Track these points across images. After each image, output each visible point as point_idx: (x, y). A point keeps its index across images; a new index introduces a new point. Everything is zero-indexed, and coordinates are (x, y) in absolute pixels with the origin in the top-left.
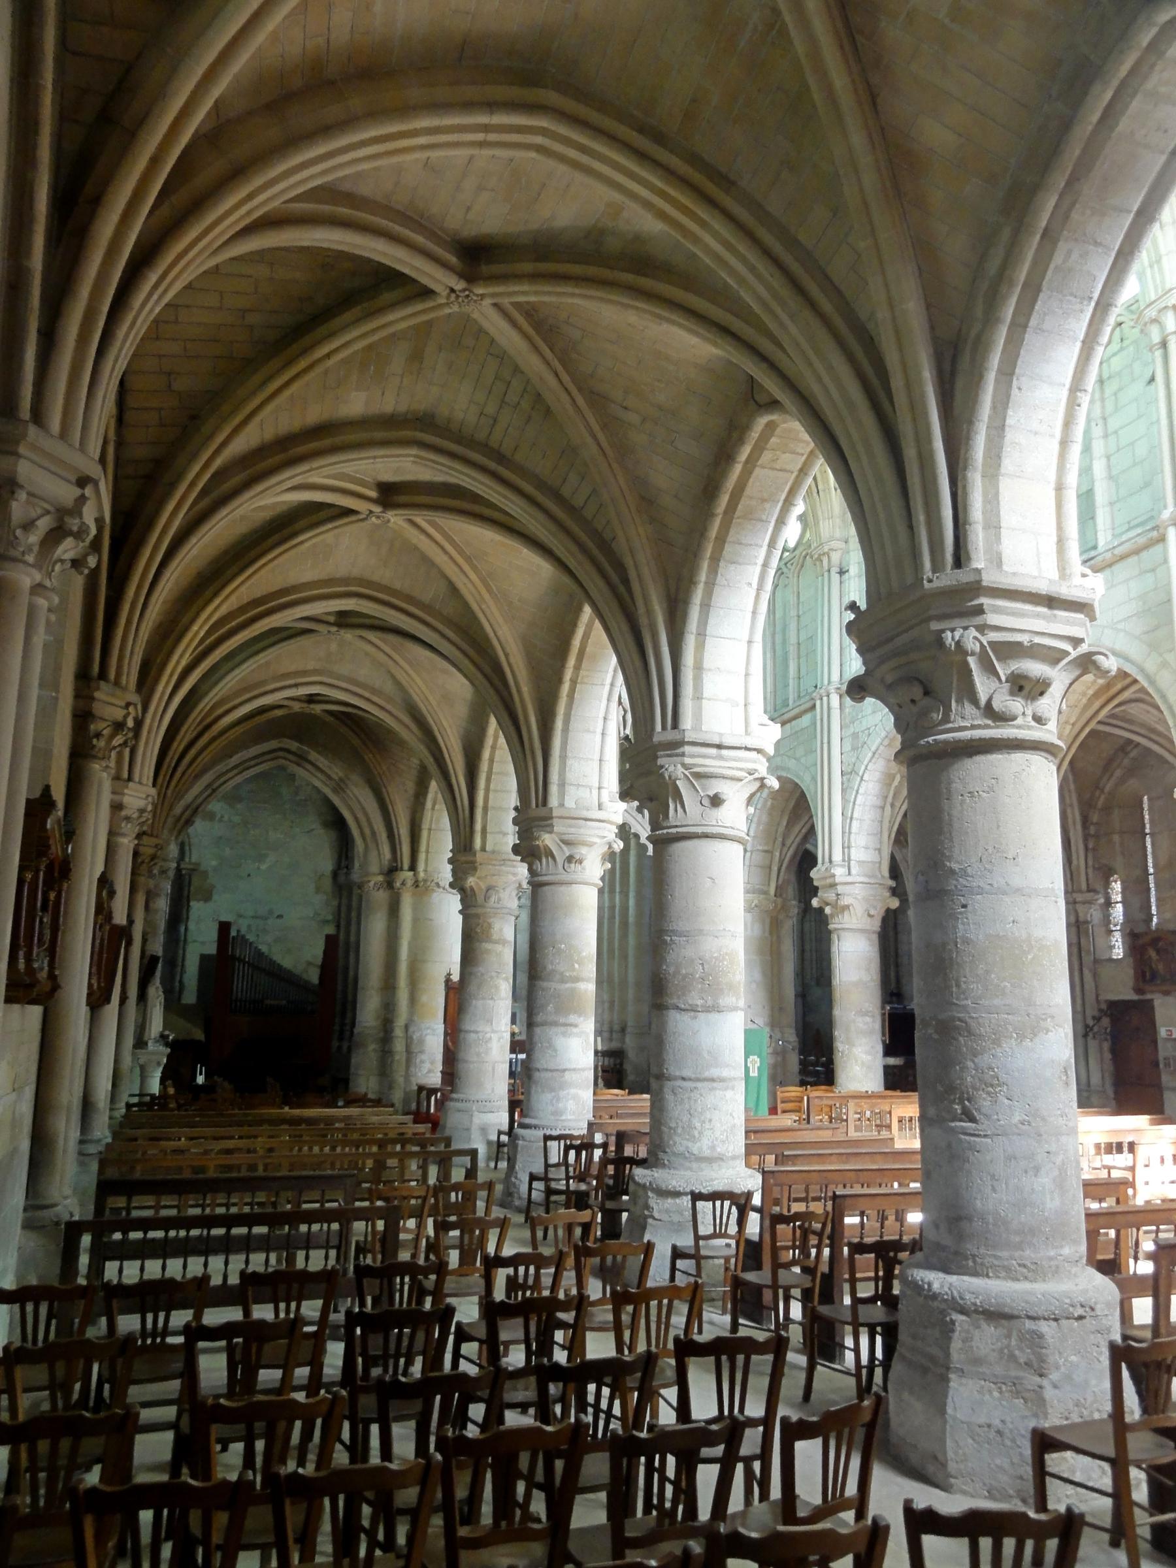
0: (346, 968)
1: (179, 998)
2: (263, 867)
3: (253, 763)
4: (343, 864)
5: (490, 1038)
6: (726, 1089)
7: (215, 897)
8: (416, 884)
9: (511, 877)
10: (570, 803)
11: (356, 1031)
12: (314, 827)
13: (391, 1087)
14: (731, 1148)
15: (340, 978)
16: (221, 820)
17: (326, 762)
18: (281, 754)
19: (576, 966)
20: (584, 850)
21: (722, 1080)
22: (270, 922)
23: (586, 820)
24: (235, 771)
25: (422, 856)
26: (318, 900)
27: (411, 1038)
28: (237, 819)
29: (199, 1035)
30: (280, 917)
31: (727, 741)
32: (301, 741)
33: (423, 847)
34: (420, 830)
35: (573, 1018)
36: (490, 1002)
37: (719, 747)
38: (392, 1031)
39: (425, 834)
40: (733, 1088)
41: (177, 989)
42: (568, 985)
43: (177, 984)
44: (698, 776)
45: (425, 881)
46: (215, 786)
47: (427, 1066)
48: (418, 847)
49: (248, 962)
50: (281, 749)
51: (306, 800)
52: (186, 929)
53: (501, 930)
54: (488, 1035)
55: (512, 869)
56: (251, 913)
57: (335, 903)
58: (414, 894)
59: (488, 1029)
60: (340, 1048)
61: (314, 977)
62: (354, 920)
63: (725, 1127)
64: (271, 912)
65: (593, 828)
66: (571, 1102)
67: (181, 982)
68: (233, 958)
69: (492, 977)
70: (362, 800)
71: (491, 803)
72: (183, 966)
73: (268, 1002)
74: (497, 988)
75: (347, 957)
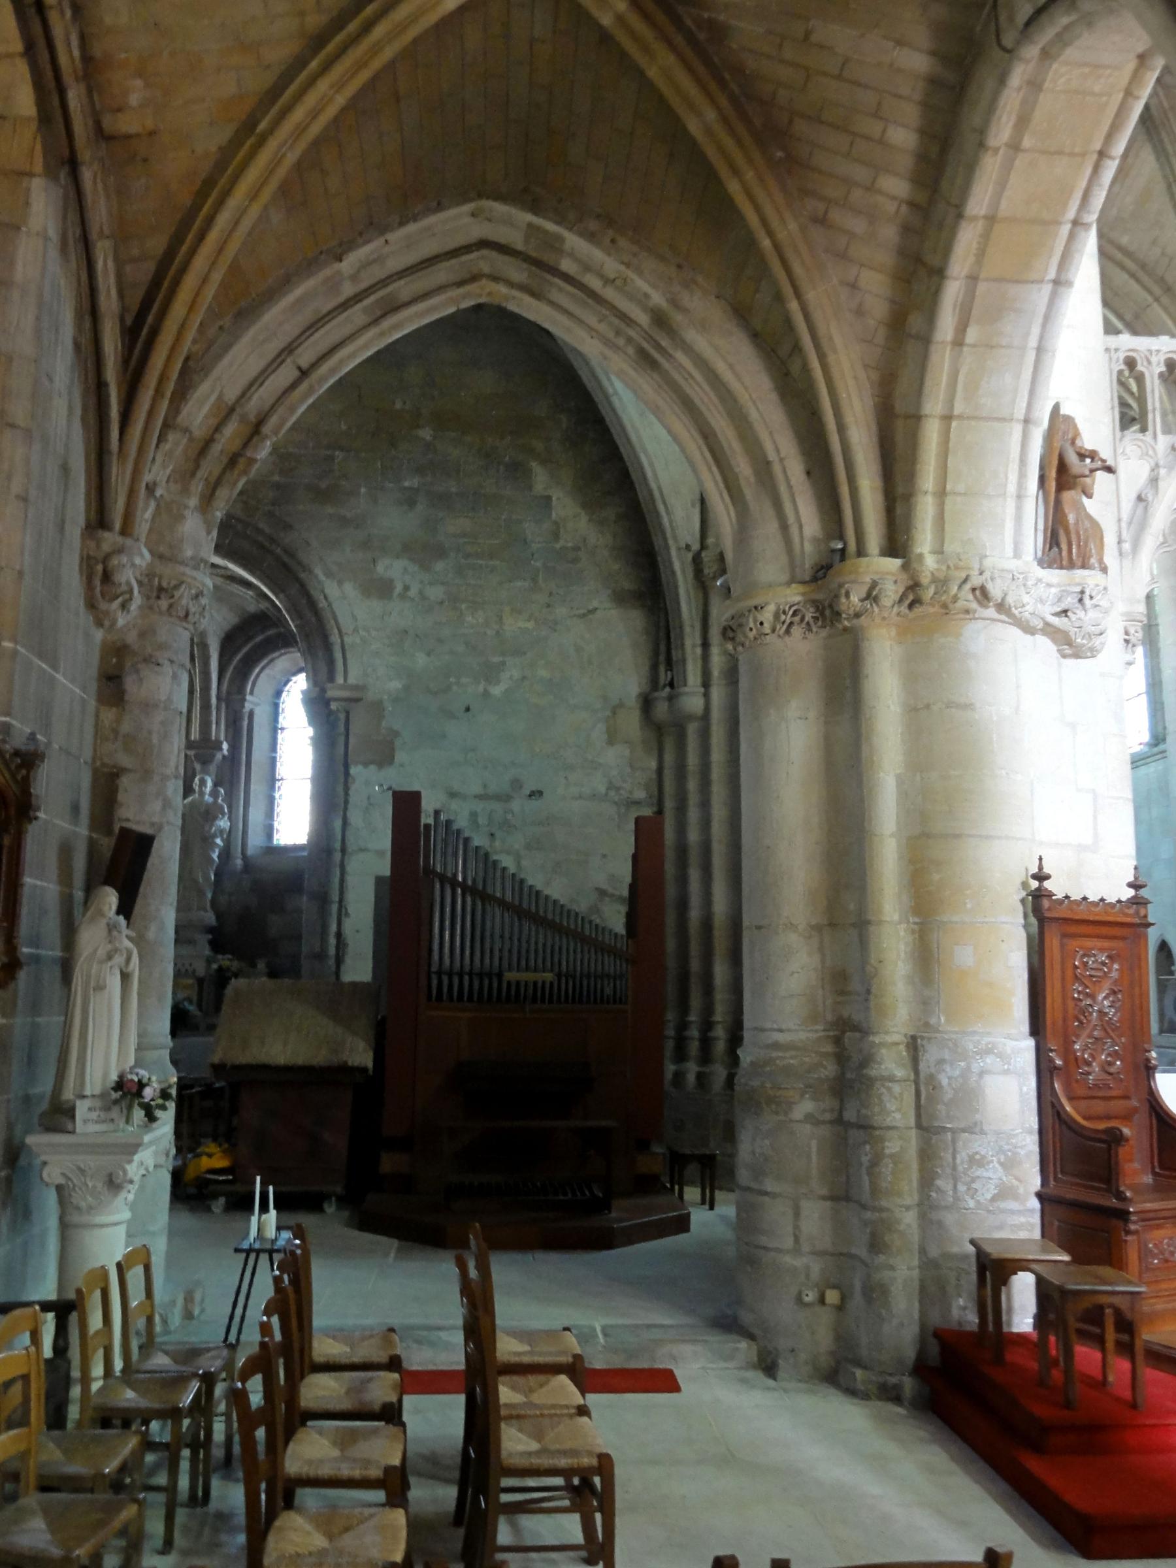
0: (683, 905)
1: (337, 974)
2: (497, 691)
3: (404, 289)
4: (663, 677)
7: (400, 756)
8: (912, 595)
11: (746, 1055)
12: (595, 604)
13: (876, 1245)
15: (670, 919)
16: (403, 596)
17: (611, 266)
18: (483, 261)
22: (516, 805)
24: (357, 315)
25: (925, 509)
26: (614, 757)
27: (931, 1078)
28: (436, 593)
29: (361, 1055)
30: (536, 794)
32: (535, 207)
33: (927, 480)
34: (916, 418)
38: (867, 1061)
39: (931, 433)
41: (332, 951)
43: (332, 941)
45: (942, 583)
46: (305, 357)
47: (992, 1175)
48: (911, 476)
49: (463, 885)
50: (484, 244)
51: (577, 549)
52: (345, 823)
56: (477, 789)
57: (654, 764)
58: (904, 632)
60: (679, 1077)
61: (615, 919)
62: (693, 799)
64: (517, 784)
67: (339, 935)
68: (429, 872)
70: (721, 367)
72: (341, 901)
73: (511, 976)
75: (683, 880)
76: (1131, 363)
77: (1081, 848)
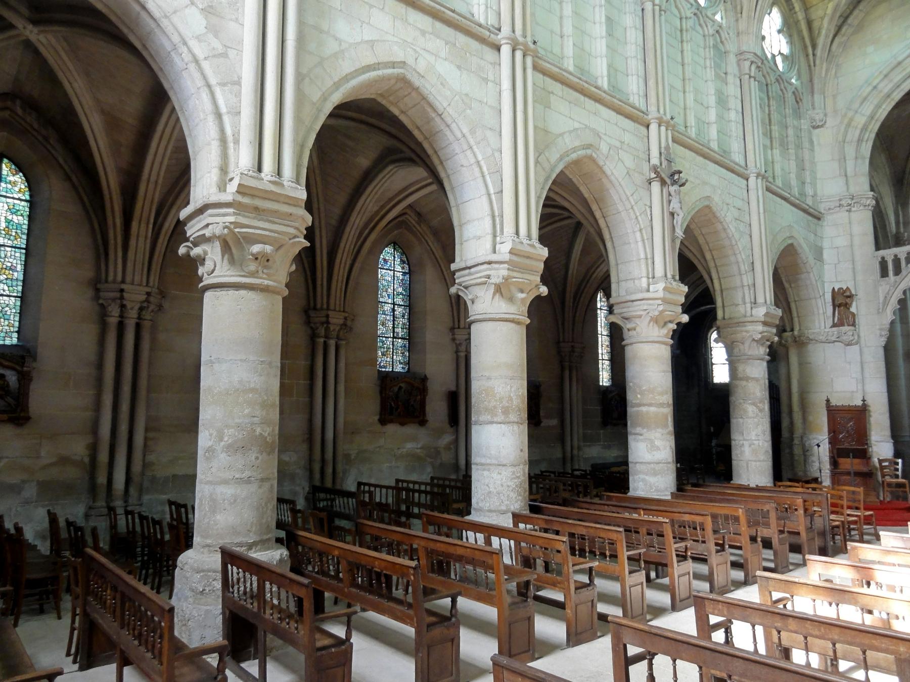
5: (743, 444)
6: (484, 470)
9: (744, 334)
10: (622, 293)
19: (639, 396)
20: (637, 321)
21: (482, 464)
23: (633, 301)
31: (469, 264)
35: (638, 430)
36: (741, 420)
37: (470, 268)
40: (489, 470)
42: (635, 409)
44: (466, 288)
45: (799, 337)
47: (816, 465)
53: (744, 371)
54: (741, 442)
55: (744, 329)
59: (741, 438)
63: (483, 492)
65: (637, 306)
66: (641, 483)
69: (740, 404)
71: (723, 287)
74: (745, 411)
76: (883, 258)
77: (853, 392)
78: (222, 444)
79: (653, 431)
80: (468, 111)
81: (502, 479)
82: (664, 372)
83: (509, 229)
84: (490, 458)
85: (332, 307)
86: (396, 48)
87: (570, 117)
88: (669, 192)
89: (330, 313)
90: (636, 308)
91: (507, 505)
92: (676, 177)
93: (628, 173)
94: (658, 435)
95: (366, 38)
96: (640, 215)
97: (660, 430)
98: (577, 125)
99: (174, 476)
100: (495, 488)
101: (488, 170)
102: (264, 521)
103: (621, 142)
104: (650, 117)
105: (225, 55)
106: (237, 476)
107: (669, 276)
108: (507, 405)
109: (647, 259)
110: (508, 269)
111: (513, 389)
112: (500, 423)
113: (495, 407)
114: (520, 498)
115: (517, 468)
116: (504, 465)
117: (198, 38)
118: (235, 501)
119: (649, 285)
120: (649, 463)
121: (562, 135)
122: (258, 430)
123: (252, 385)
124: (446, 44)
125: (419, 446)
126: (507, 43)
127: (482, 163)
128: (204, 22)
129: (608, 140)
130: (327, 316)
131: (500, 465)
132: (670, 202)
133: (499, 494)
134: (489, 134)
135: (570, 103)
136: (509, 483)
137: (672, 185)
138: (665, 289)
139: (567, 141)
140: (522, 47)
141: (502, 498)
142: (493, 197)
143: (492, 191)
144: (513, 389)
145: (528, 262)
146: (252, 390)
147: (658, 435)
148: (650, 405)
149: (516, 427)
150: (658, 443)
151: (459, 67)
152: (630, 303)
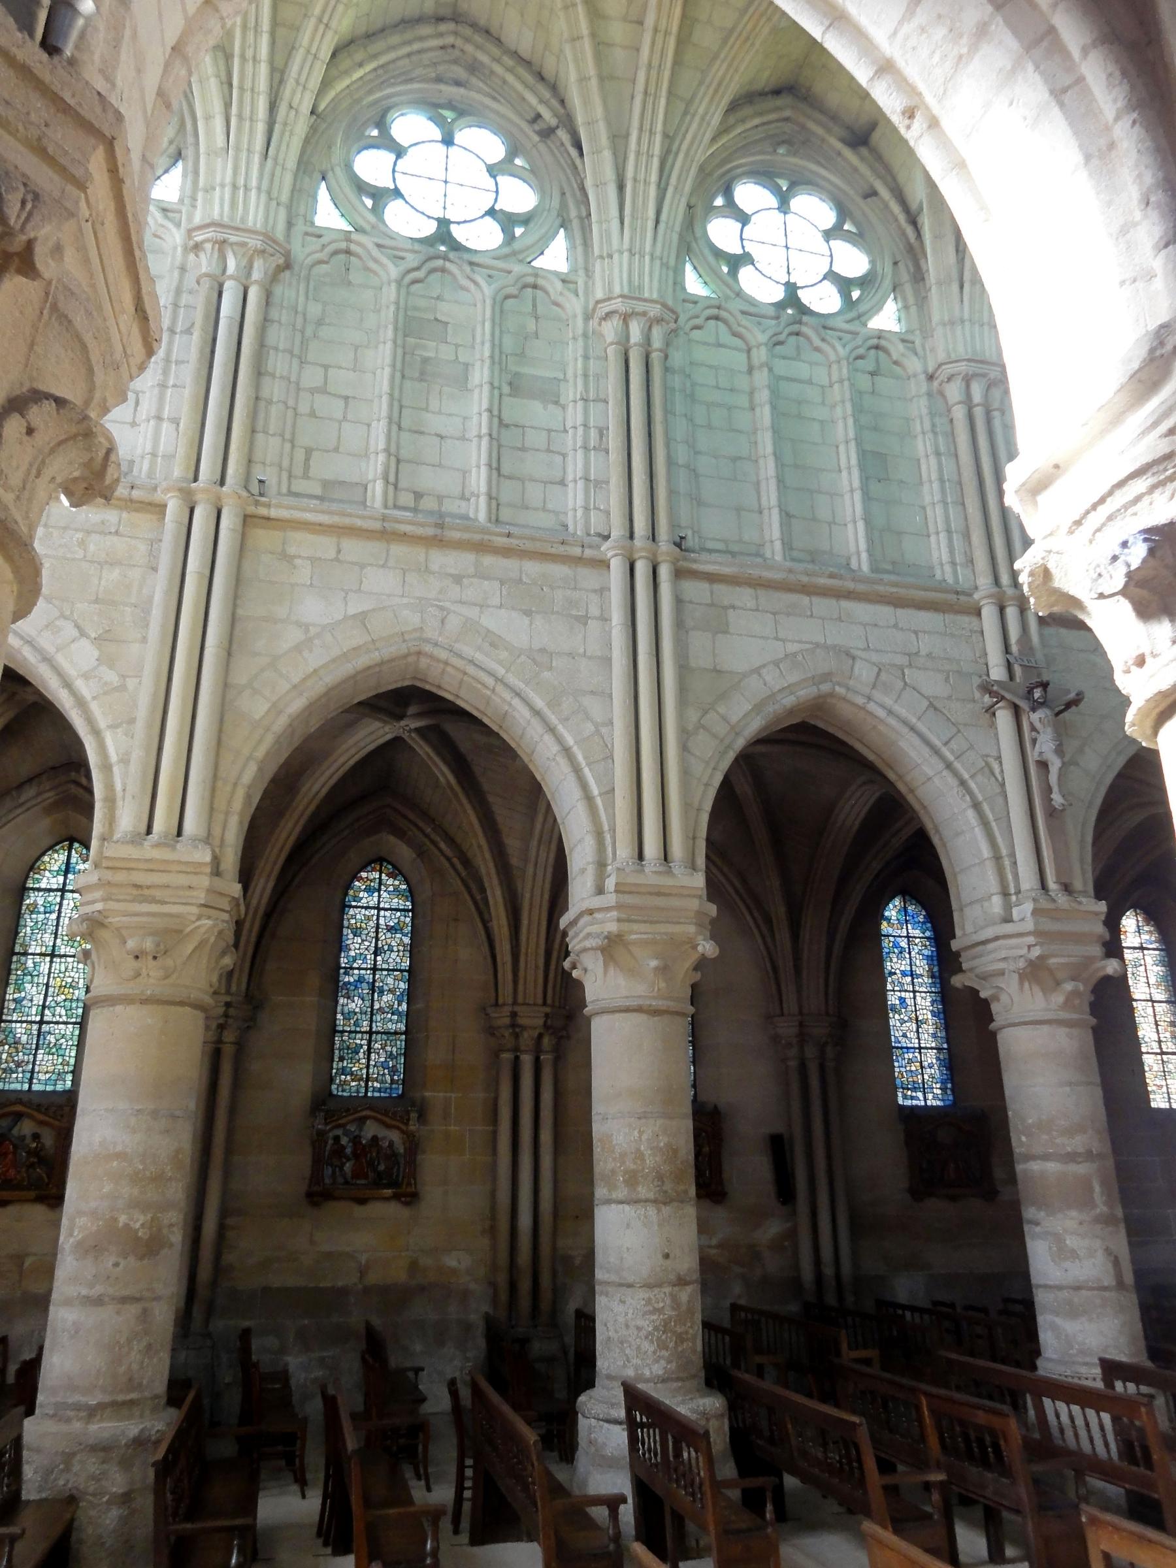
14: (606, 1364)
19: (1024, 1139)
78: (72, 1240)
79: (1060, 1216)
80: (546, 674)
81: (626, 1314)
82: (1070, 1084)
83: (624, 851)
84: (608, 1272)
85: (520, 1000)
86: (406, 612)
87: (777, 639)
88: (1031, 724)
89: (517, 1009)
90: (990, 957)
91: (636, 1368)
92: (1037, 694)
93: (931, 705)
94: (1071, 1224)
95: (352, 611)
96: (972, 777)
97: (1074, 1213)
98: (792, 648)
99: (266, 1290)
100: (616, 1332)
101: (585, 758)
102: (122, 1369)
103: (909, 655)
104: (976, 596)
105: (122, 688)
106: (84, 1292)
107: (1052, 885)
108: (632, 1166)
109: (997, 858)
110: (619, 920)
111: (644, 1137)
112: (621, 1202)
113: (613, 1171)
114: (665, 1353)
115: (656, 1290)
116: (630, 1286)
117: (86, 676)
118: (76, 1332)
119: (1008, 907)
120: (1060, 1288)
121: (757, 671)
122: (123, 1219)
123: (119, 1148)
124: (502, 583)
125: (714, 1242)
126: (616, 555)
127: (575, 749)
128: (96, 653)
129: (875, 657)
130: (514, 1015)
131: (621, 1285)
132: (1034, 741)
133: (622, 1343)
134: (587, 701)
135: (774, 614)
136: (640, 1323)
137: (1034, 710)
138: (1035, 912)
139: (768, 678)
140: (643, 554)
141: (628, 1351)
142: (599, 801)
143: (595, 791)
144: (644, 1137)
145: (660, 902)
146: (120, 1156)
147: (1071, 1224)
148: (1046, 1157)
149: (652, 1211)
150: (1071, 1242)
151: (528, 613)
152: (980, 948)
